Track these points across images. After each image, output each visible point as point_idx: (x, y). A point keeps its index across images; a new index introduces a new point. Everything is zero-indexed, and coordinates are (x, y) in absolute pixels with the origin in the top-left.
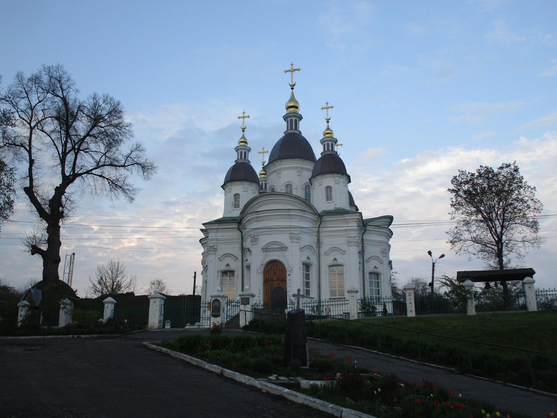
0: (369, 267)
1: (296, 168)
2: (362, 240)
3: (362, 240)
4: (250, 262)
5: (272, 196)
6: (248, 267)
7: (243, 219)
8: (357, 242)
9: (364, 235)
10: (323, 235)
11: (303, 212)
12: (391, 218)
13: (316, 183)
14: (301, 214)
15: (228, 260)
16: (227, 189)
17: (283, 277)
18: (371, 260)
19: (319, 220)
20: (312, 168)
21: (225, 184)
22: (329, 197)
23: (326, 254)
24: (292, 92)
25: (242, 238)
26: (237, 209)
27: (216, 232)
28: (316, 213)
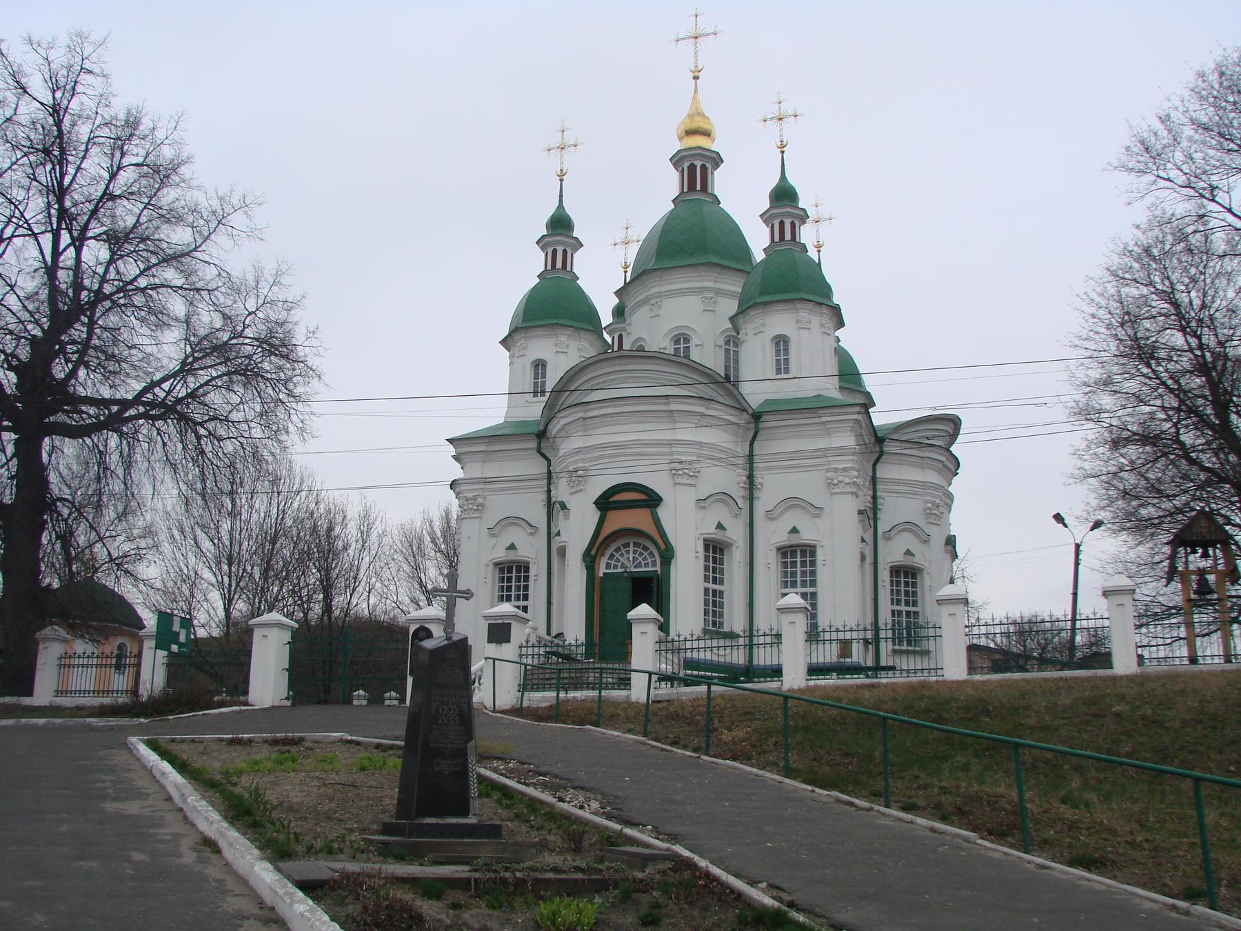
0: (892, 553)
1: (702, 290)
2: (874, 479)
3: (874, 479)
4: (567, 540)
5: (626, 361)
6: (562, 552)
7: (550, 427)
8: (854, 483)
9: (878, 465)
12: (954, 423)
13: (749, 329)
14: (702, 410)
15: (516, 535)
16: (516, 349)
18: (896, 534)
19: (753, 425)
20: (740, 290)
21: (509, 336)
22: (782, 366)
23: (770, 516)
25: (549, 473)
27: (484, 462)
28: (741, 404)
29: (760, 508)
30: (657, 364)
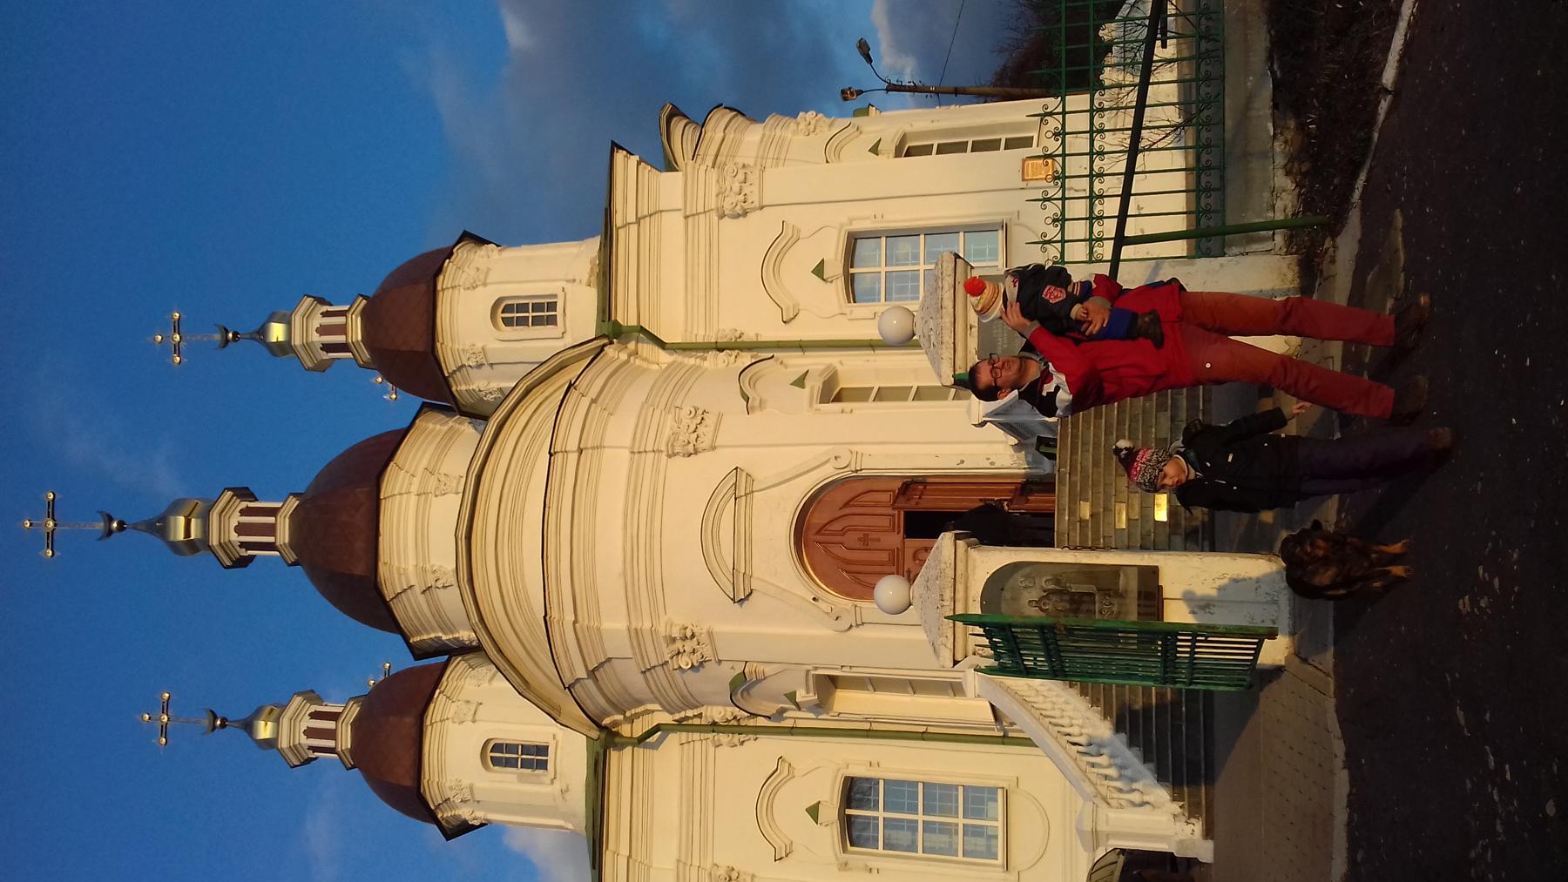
10: (702, 332)
11: (574, 394)
17: (885, 497)
24: (135, 527)
26: (550, 758)
29: (774, 331)
30: (493, 475)
